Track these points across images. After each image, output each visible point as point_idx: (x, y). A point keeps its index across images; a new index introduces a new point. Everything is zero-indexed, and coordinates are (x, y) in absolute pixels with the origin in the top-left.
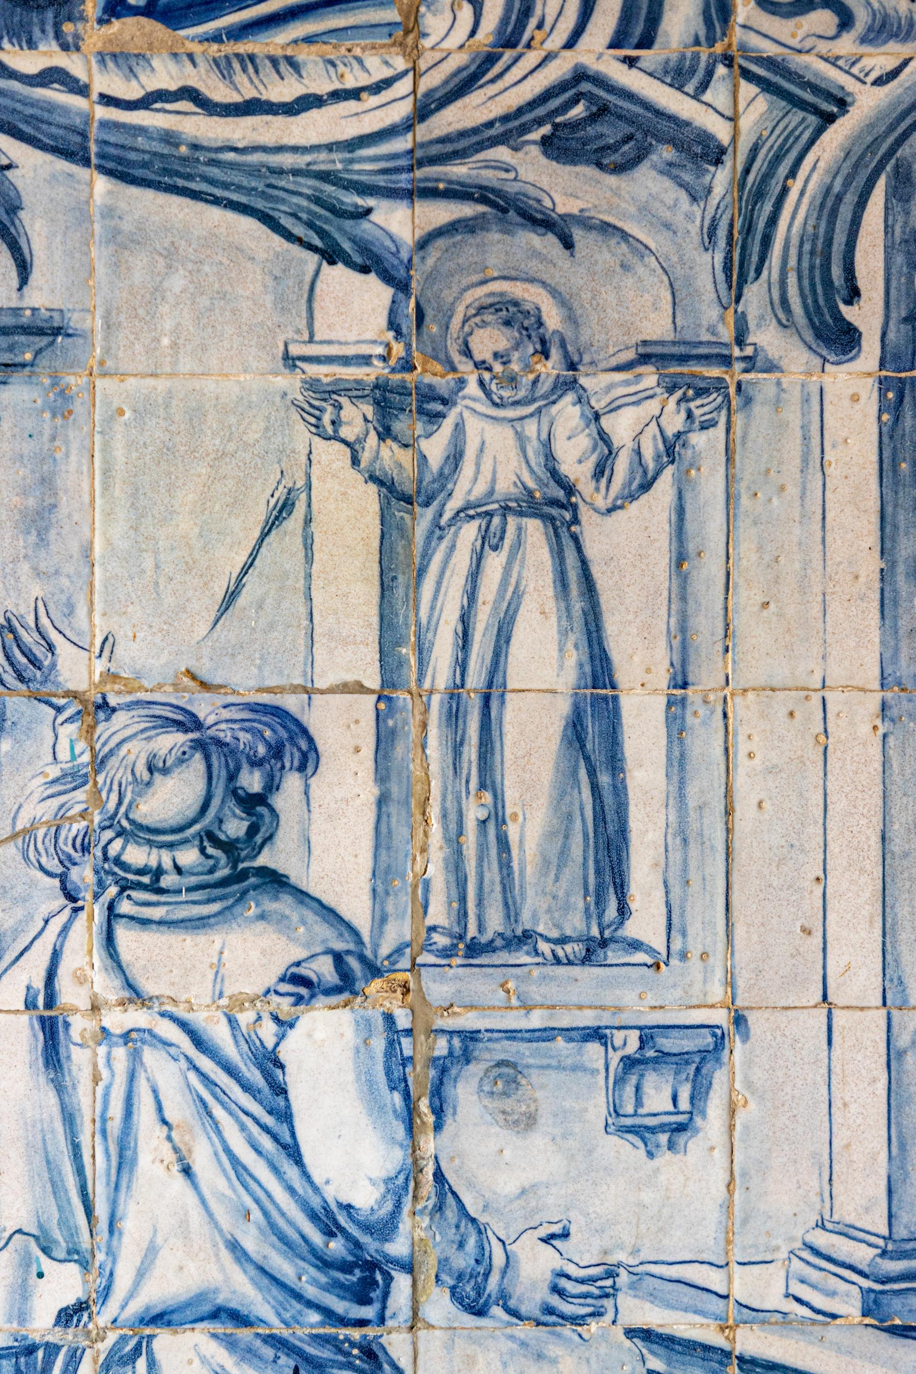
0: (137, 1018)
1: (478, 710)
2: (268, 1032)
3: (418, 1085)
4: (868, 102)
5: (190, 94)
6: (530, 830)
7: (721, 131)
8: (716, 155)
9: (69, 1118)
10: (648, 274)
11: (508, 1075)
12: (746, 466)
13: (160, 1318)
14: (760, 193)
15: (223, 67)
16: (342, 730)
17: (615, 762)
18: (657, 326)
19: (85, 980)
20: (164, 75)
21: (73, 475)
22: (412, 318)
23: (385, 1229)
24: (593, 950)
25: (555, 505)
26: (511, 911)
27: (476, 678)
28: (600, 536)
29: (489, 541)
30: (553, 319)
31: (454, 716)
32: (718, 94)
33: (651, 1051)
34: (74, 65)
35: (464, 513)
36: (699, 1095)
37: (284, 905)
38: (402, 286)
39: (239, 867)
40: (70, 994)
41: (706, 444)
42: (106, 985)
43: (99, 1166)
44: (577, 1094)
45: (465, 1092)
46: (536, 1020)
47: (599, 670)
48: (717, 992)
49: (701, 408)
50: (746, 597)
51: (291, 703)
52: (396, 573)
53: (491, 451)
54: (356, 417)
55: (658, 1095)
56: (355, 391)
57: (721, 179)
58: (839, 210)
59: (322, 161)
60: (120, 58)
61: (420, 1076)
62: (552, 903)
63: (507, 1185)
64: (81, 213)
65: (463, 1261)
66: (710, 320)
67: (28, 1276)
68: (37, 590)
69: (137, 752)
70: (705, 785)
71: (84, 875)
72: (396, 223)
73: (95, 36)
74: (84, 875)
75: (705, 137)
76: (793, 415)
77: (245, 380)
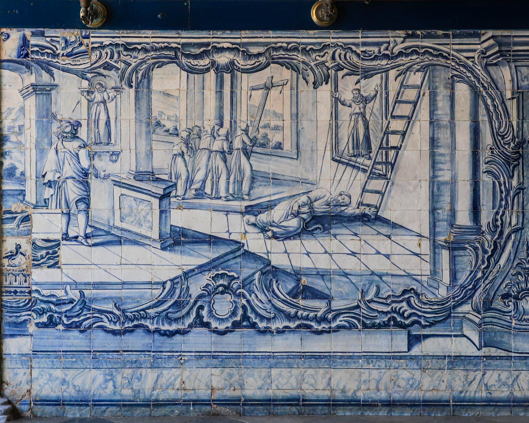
0: (65, 150)
1: (97, 122)
2: (77, 151)
3: (91, 157)
4: (133, 65)
5: (70, 64)
6: (102, 132)
7: (120, 67)
9: (59, 160)
11: (100, 156)
12: (122, 98)
13: (67, 178)
14: (123, 73)
15: (73, 61)
16: (84, 123)
17: (110, 126)
18: (114, 85)
19: (60, 146)
20: (67, 62)
21: (59, 99)
22: (90, 85)
23: (88, 170)
24: (108, 144)
25: (104, 102)
26: (100, 140)
27: (97, 118)
28: (108, 105)
29: (98, 105)
30: (104, 85)
31: (95, 122)
32: (119, 63)
34: (59, 61)
35: (96, 103)
36: (118, 158)
37: (79, 139)
38: (90, 81)
39: (74, 136)
40: (58, 148)
41: (118, 96)
43: (61, 164)
44: (106, 158)
45: (96, 157)
46: (102, 151)
47: (108, 117)
48: (120, 148)
49: (118, 93)
50: (122, 111)
51: (79, 121)
52: (89, 108)
53: (98, 97)
54: (85, 94)
55: (114, 158)
56: (85, 91)
57: (120, 72)
58: (131, 74)
59: (82, 70)
60: (63, 60)
61: (91, 156)
62: (104, 140)
63: (100, 166)
64: (60, 75)
65: (96, 173)
66: (119, 85)
67: (55, 174)
68: (55, 110)
69: (65, 125)
70: (118, 129)
71: (60, 137)
72: (89, 76)
73: (61, 58)
74: (60, 137)
75: (118, 68)
76: (127, 94)
77: (75, 91)
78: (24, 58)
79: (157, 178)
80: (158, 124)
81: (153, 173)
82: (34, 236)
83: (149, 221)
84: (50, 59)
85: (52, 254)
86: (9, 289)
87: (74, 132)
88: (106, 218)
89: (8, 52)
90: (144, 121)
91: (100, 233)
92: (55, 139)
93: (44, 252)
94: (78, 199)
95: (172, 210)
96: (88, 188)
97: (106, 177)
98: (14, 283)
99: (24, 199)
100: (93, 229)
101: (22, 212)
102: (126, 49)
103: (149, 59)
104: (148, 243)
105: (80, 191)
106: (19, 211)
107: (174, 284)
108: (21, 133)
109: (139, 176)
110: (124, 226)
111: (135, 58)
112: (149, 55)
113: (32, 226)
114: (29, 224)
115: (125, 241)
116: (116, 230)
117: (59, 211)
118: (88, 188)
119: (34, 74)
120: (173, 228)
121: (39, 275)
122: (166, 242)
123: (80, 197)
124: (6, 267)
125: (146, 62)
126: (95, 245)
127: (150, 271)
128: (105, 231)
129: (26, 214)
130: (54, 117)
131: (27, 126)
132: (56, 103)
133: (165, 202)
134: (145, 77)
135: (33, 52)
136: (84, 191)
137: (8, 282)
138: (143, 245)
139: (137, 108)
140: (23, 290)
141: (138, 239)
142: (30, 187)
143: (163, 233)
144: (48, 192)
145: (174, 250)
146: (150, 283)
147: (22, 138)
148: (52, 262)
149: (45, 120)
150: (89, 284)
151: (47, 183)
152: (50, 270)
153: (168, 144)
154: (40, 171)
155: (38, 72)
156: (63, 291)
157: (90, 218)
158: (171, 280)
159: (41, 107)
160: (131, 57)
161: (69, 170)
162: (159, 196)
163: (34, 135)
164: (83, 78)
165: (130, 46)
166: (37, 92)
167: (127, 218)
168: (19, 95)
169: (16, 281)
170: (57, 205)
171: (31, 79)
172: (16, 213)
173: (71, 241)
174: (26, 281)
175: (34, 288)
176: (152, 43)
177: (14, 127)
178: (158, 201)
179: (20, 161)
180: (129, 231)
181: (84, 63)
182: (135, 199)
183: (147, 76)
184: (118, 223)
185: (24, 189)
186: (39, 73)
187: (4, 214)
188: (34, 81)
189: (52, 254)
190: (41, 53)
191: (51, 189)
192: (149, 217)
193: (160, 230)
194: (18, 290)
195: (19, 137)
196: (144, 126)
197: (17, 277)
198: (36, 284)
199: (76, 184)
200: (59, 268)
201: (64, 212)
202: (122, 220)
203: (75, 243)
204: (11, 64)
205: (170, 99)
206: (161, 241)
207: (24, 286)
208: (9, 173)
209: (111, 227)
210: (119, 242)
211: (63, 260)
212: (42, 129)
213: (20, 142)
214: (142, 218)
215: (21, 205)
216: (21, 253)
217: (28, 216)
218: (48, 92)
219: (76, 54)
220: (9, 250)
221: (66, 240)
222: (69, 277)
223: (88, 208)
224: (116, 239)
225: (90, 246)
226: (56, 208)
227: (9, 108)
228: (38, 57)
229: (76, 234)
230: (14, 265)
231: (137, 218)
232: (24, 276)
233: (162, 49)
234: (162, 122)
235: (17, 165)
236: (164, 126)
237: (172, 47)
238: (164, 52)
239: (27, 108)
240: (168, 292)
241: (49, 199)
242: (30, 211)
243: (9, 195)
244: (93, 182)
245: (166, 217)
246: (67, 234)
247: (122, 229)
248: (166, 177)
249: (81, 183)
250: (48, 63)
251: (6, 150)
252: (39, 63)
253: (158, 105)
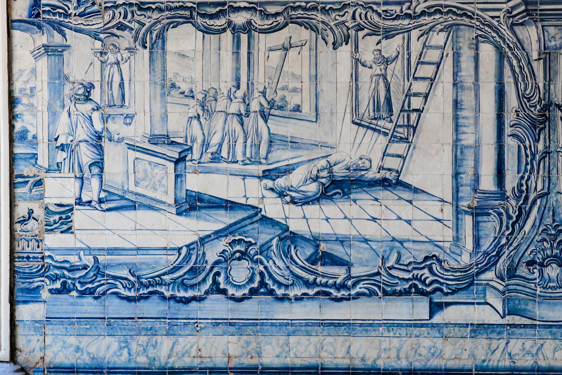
0: (78, 113)
1: (110, 84)
3: (105, 119)
4: (148, 25)
8: (133, 29)
9: (71, 123)
10: (126, 41)
11: (113, 118)
13: (80, 141)
14: (137, 33)
15: (85, 21)
17: (124, 88)
18: (128, 46)
19: (73, 109)
20: (80, 22)
21: (71, 59)
22: (104, 45)
23: (102, 133)
24: (122, 106)
25: (118, 63)
26: (114, 103)
27: (110, 80)
28: (121, 66)
29: (111, 67)
30: (117, 45)
31: (108, 84)
32: (133, 23)
33: (127, 116)
38: (103, 42)
39: (88, 99)
41: (132, 57)
42: (75, 109)
44: (120, 120)
45: (109, 120)
46: (116, 113)
47: (122, 79)
49: (132, 54)
51: (92, 82)
53: (111, 58)
54: (98, 55)
55: (128, 121)
56: (98, 52)
58: (145, 35)
60: (75, 20)
61: (105, 119)
62: (118, 102)
63: (113, 129)
64: (72, 35)
65: (109, 136)
66: (133, 46)
69: (77, 87)
70: (132, 91)
71: (72, 99)
72: (102, 36)
73: (73, 18)
74: (72, 99)
78: (36, 17)
79: (173, 142)
80: (173, 86)
81: (168, 136)
82: (47, 201)
83: (164, 186)
84: (62, 19)
85: (65, 219)
86: (21, 255)
87: (87, 94)
88: (120, 182)
89: (19, 12)
90: (159, 83)
91: (114, 198)
92: (67, 101)
93: (57, 217)
94: (91, 162)
95: (187, 174)
96: (101, 152)
97: (120, 140)
98: (27, 248)
99: (36, 163)
100: (106, 194)
101: (35, 176)
102: (140, 9)
103: (164, 19)
104: (163, 208)
105: (94, 154)
106: (32, 175)
107: (190, 250)
108: (33, 96)
109: (154, 139)
110: (139, 190)
111: (149, 17)
112: (164, 14)
113: (44, 190)
114: (42, 189)
115: (139, 206)
116: (130, 194)
117: (73, 175)
118: (101, 152)
119: (45, 35)
120: (188, 192)
121: (53, 240)
122: (182, 206)
123: (93, 161)
124: (18, 232)
125: (160, 22)
127: (166, 236)
128: (119, 196)
129: (38, 178)
130: (67, 78)
131: (39, 88)
132: (68, 65)
133: (181, 166)
134: (159, 38)
135: (44, 12)
136: (98, 155)
137: (21, 248)
138: (158, 210)
139: (152, 69)
140: (36, 255)
141: (153, 204)
143: (178, 198)
144: (61, 156)
145: (190, 216)
146: (165, 249)
147: (34, 101)
148: (65, 227)
149: (57, 82)
150: (103, 250)
151: (60, 147)
152: (63, 235)
153: (183, 106)
154: (53, 134)
155: (49, 32)
156: (77, 257)
157: (103, 183)
159: (53, 68)
160: (145, 17)
161: (82, 133)
162: (175, 160)
164: (96, 39)
165: (144, 5)
166: (49, 53)
167: (142, 183)
168: (31, 56)
169: (28, 247)
170: (70, 169)
172: (28, 177)
173: (85, 205)
174: (38, 247)
175: (47, 253)
176: (167, 2)
177: (25, 89)
178: (172, 165)
179: (32, 124)
180: (144, 196)
181: (96, 23)
182: (150, 163)
183: (162, 36)
184: (132, 188)
185: (36, 152)
186: (51, 33)
187: (16, 178)
188: (45, 42)
189: (65, 219)
190: (53, 13)
191: (63, 152)
192: (164, 182)
193: (175, 195)
194: (31, 255)
195: (30, 99)
196: (158, 87)
197: (30, 242)
198: (49, 250)
199: (89, 147)
200: (72, 233)
201: (78, 176)
202: (136, 184)
203: (89, 208)
204: (22, 24)
205: (186, 60)
206: (176, 206)
207: (37, 251)
208: (21, 136)
210: (133, 207)
211: (76, 225)
212: (55, 91)
213: (32, 104)
214: (157, 183)
215: (34, 168)
216: (34, 218)
217: (40, 180)
218: (60, 53)
219: (89, 14)
220: (21, 215)
221: (79, 205)
222: (82, 243)
223: (102, 172)
224: (130, 204)
225: (104, 211)
226: (69, 172)
227: (20, 70)
228: (49, 17)
229: (89, 199)
230: (26, 230)
231: (152, 183)
232: (37, 241)
233: (177, 8)
234: (178, 84)
235: (29, 128)
236: (179, 88)
237: (187, 6)
238: (179, 12)
239: (39, 70)
240: (184, 258)
241: (61, 163)
242: (42, 175)
243: (21, 159)
245: (181, 181)
246: (80, 199)
247: (137, 194)
248: (181, 141)
249: (94, 146)
250: (60, 24)
251: (17, 113)
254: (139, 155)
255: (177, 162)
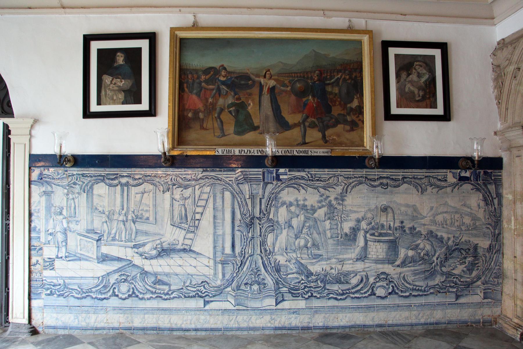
3: (68, 223)
4: (86, 183)
6: (72, 212)
14: (82, 186)
16: (65, 208)
22: (68, 191)
39: (61, 213)
44: (74, 223)
52: (67, 201)
53: (71, 196)
55: (78, 223)
58: (85, 187)
66: (80, 191)
72: (67, 187)
80: (96, 209)
82: (44, 256)
92: (53, 215)
102: (83, 176)
109: (89, 231)
110: (82, 252)
121: (47, 273)
126: (69, 261)
130: (53, 205)
133: (99, 242)
138: (90, 261)
141: (87, 258)
142: (43, 235)
144: (50, 238)
146: (93, 277)
148: (52, 268)
158: (102, 276)
161: (58, 229)
163: (44, 213)
171: (44, 189)
175: (44, 279)
182: (86, 241)
183: (92, 187)
184: (79, 252)
192: (92, 249)
196: (90, 209)
209: (76, 253)
210: (80, 259)
233: (98, 176)
234: (98, 208)
239: (41, 201)
242: (42, 246)
244: (69, 234)
246: (58, 256)
250: (49, 182)
252: (46, 182)
253: (96, 200)
254: (82, 238)
255: (97, 241)
